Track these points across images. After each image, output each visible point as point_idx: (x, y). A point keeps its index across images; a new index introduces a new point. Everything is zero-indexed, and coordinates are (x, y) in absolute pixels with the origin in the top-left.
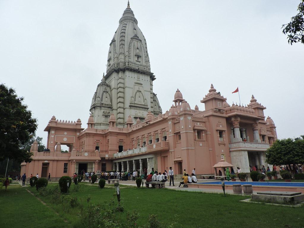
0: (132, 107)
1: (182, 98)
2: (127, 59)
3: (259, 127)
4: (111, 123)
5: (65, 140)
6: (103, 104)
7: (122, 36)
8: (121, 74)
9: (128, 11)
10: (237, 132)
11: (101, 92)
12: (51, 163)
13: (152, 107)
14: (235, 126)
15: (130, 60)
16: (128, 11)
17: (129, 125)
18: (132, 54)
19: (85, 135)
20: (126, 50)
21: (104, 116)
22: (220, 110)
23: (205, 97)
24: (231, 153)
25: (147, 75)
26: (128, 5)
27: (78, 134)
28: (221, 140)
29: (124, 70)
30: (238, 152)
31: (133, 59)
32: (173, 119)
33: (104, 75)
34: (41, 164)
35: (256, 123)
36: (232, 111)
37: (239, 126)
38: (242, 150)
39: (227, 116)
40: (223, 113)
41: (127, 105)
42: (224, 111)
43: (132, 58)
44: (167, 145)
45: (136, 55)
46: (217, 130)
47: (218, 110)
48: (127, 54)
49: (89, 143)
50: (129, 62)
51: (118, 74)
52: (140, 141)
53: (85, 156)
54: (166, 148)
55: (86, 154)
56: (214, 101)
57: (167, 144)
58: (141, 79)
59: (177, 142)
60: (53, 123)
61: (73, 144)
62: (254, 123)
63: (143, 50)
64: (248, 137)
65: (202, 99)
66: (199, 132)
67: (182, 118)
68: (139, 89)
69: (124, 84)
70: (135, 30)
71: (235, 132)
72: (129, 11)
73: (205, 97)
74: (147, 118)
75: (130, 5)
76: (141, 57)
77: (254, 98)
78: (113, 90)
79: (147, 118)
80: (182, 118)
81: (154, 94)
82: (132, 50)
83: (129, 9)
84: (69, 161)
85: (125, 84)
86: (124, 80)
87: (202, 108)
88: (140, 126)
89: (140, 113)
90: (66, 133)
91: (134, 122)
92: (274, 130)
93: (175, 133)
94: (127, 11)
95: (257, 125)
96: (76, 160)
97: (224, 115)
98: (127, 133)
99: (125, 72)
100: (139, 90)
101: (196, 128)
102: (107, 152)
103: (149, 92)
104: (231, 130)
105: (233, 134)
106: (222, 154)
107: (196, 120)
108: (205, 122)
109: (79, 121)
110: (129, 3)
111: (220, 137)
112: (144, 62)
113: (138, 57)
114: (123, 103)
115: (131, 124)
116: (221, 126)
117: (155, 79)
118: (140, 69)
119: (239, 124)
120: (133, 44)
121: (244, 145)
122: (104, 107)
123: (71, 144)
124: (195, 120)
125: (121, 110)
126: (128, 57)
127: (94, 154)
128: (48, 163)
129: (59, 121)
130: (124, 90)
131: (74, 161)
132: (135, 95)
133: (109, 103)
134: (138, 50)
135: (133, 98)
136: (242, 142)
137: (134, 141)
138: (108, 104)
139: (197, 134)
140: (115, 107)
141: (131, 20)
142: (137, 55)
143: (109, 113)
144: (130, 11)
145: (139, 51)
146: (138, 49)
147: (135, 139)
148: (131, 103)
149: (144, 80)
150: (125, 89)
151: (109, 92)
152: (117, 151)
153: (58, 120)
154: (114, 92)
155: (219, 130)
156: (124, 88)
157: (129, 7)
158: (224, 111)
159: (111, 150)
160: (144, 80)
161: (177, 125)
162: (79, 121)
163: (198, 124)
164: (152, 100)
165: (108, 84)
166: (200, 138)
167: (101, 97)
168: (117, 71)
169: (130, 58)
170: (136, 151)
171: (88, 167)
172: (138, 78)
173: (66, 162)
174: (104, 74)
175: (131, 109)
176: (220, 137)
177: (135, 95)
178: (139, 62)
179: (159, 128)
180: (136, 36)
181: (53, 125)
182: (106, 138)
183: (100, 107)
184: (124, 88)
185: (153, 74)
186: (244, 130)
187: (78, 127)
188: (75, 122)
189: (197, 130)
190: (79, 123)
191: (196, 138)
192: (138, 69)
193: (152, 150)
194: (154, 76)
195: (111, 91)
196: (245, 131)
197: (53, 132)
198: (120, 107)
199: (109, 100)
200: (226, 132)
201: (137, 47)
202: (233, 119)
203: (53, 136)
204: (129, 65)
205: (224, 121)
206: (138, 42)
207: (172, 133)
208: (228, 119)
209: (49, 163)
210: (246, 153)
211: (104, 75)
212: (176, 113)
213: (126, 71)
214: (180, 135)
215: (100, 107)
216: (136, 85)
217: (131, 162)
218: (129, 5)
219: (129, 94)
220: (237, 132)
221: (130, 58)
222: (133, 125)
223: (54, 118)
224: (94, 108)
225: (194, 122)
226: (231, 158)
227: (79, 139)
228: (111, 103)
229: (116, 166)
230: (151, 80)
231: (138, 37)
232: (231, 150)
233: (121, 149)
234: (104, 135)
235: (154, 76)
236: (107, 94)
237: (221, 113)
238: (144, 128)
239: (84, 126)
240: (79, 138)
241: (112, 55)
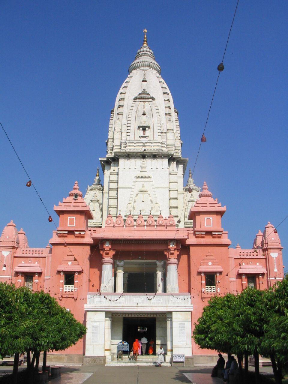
10: (105, 272)
18: (133, 127)
28: (70, 290)
35: (169, 250)
40: (83, 237)
42: (82, 233)
43: (132, 134)
45: (139, 128)
46: (59, 272)
50: (126, 143)
58: (148, 169)
62: (165, 249)
63: (155, 115)
76: (149, 127)
82: (133, 119)
112: (156, 134)
120: (135, 109)
126: (126, 134)
135: (129, 205)
145: (147, 117)
146: (144, 114)
155: (64, 272)
172: (142, 167)
192: (142, 151)
206: (147, 104)
208: (97, 247)
221: (129, 134)
231: (149, 94)
236: (97, 204)
237: (76, 237)
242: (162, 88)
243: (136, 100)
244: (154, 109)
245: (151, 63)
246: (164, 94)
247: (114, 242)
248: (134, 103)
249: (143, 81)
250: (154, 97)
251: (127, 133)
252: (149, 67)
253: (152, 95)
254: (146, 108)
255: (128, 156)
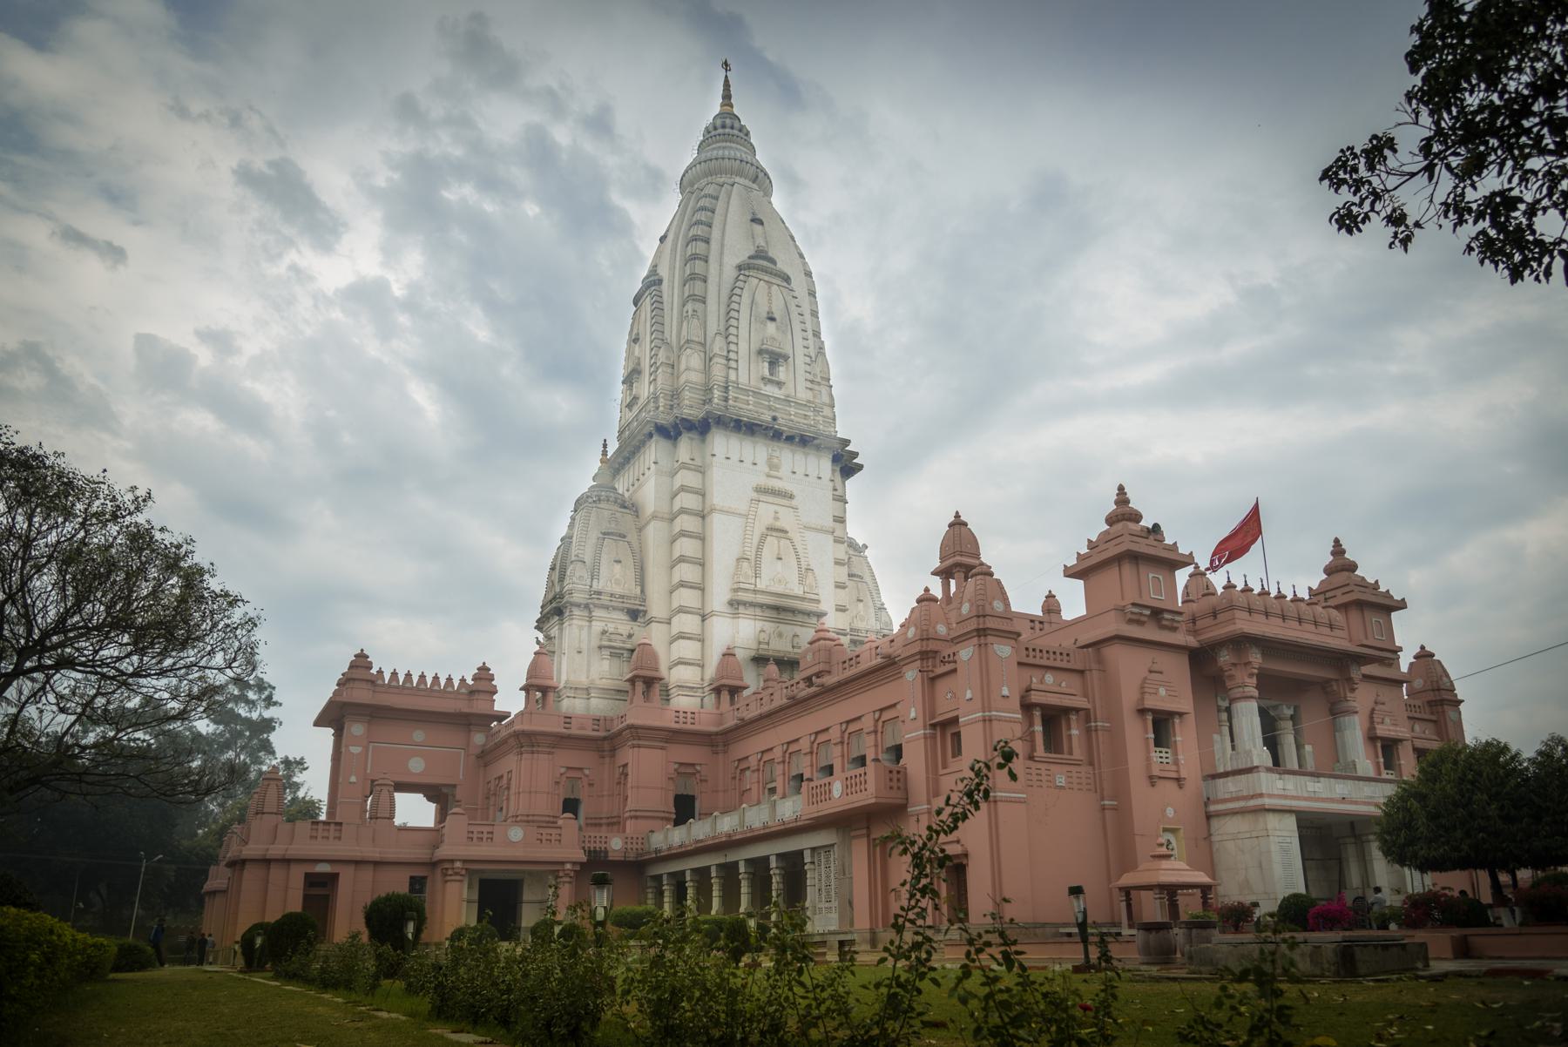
0: (741, 609)
1: (977, 556)
2: (718, 371)
3: (1362, 698)
4: (640, 686)
5: (416, 766)
6: (599, 593)
8: (686, 448)
11: (594, 535)
12: (346, 876)
13: (841, 609)
14: (1236, 693)
15: (733, 376)
17: (725, 696)
19: (512, 742)
20: (713, 325)
21: (606, 652)
22: (1156, 613)
23: (1084, 550)
24: (1215, 823)
25: (818, 448)
27: (479, 739)
29: (702, 428)
30: (1249, 817)
31: (748, 372)
32: (925, 655)
33: (605, 453)
34: (297, 875)
36: (1221, 617)
37: (1256, 693)
38: (1269, 810)
39: (1192, 641)
40: (1174, 629)
41: (719, 595)
43: (743, 365)
44: (895, 784)
45: (760, 352)
47: (1148, 612)
48: (718, 346)
49: (532, 781)
51: (675, 446)
52: (779, 769)
53: (513, 842)
54: (894, 797)
55: (516, 834)
56: (1128, 569)
57: (895, 776)
58: (785, 470)
59: (945, 767)
60: (357, 684)
61: (454, 786)
63: (797, 327)
64: (1308, 748)
65: (1072, 561)
66: (1054, 718)
67: (966, 653)
68: (777, 519)
69: (703, 495)
71: (1235, 721)
73: (1084, 550)
74: (809, 657)
76: (786, 358)
77: (1344, 552)
78: (648, 523)
79: (809, 657)
80: (966, 653)
81: (852, 544)
84: (433, 865)
85: (708, 496)
86: (703, 473)
87: (1074, 603)
88: (776, 697)
89: (780, 635)
90: (419, 735)
91: (751, 680)
92: (1451, 714)
93: (933, 726)
95: (1353, 690)
96: (465, 861)
97: (1180, 638)
98: (717, 734)
99: (709, 437)
100: (778, 524)
101: (1035, 698)
102: (615, 823)
103: (826, 532)
104: (1219, 711)
105: (1226, 730)
106: (1165, 830)
107: (1037, 661)
108: (1082, 672)
109: (484, 674)
111: (1157, 745)
113: (775, 359)
114: (701, 588)
115: (734, 691)
116: (1162, 691)
117: (860, 467)
118: (780, 421)
119: (1254, 681)
120: (746, 300)
121: (1280, 784)
122: (607, 608)
123: (445, 790)
124: (1031, 660)
125: (688, 623)
127: (553, 831)
128: (334, 877)
129: (387, 677)
130: (704, 526)
131: (458, 864)
132: (759, 548)
133: (630, 587)
134: (771, 327)
135: (745, 564)
136: (1268, 770)
137: (748, 773)
138: (626, 592)
139: (1038, 728)
140: (657, 608)
142: (767, 352)
143: (630, 636)
146: (772, 319)
147: (753, 761)
148: (736, 590)
149: (800, 471)
150: (708, 520)
151: (632, 537)
152: (667, 819)
153: (380, 672)
154: (655, 534)
155: (1154, 711)
156: (703, 517)
158: (1178, 618)
159: (636, 817)
160: (800, 471)
161: (942, 686)
162: (484, 674)
163: (1049, 678)
164: (844, 570)
165: (627, 495)
166: (1058, 750)
167: (588, 558)
168: (670, 432)
169: (733, 364)
170: (756, 817)
171: (525, 898)
173: (418, 873)
174: (605, 446)
175: (735, 616)
176: (1157, 745)
177: (759, 548)
178: (779, 384)
179: (864, 704)
181: (361, 695)
182: (613, 756)
183: (587, 606)
184: (703, 517)
185: (847, 442)
186: (1289, 712)
187: (479, 707)
188: (463, 680)
189: (1044, 708)
190: (482, 686)
191: (1033, 748)
193: (826, 808)
194: (856, 455)
195: (640, 530)
196: (1292, 718)
197: (356, 729)
198: (682, 610)
199: (631, 574)
200: (1191, 720)
202: (1225, 658)
203: (355, 750)
204: (726, 400)
205: (1177, 670)
207: (920, 722)
209: (334, 877)
210: (1291, 822)
211: (605, 453)
212: (942, 629)
213: (714, 429)
214: (957, 735)
215: (587, 606)
216: (763, 498)
217: (729, 870)
219: (726, 540)
220: (1248, 717)
222: (746, 693)
223: (361, 662)
224: (559, 612)
225: (1027, 672)
226: (1216, 846)
227: (486, 765)
228: (642, 591)
229: (661, 894)
230: (838, 475)
232: (1212, 808)
233: (684, 810)
234: (606, 746)
235: (856, 455)
238: (796, 705)
239: (510, 700)
240: (486, 757)
241: (644, 351)
247: (1269, 646)
251: (728, 360)
255: (747, 428)
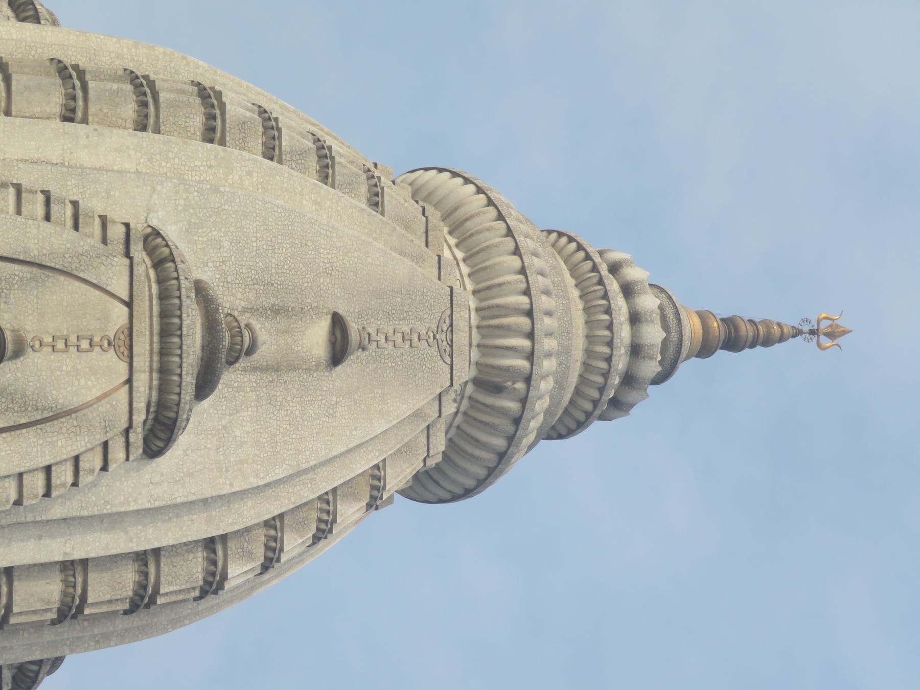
7: (144, 89)
9: (628, 290)
16: (628, 290)
26: (729, 322)
70: (315, 338)
72: (620, 304)
75: (722, 356)
83: (653, 334)
94: (620, 304)
110: (767, 337)
141: (490, 318)
144: (635, 319)
157: (692, 326)
180: (225, 350)
201: (30, 327)
218: (733, 337)
231: (205, 385)
242: (274, 524)
243: (150, 250)
244: (55, 446)
245: (524, 401)
246: (210, 544)
248: (116, 232)
249: (338, 322)
250: (183, 440)
252: (477, 382)
253: (203, 421)
254: (69, 361)
